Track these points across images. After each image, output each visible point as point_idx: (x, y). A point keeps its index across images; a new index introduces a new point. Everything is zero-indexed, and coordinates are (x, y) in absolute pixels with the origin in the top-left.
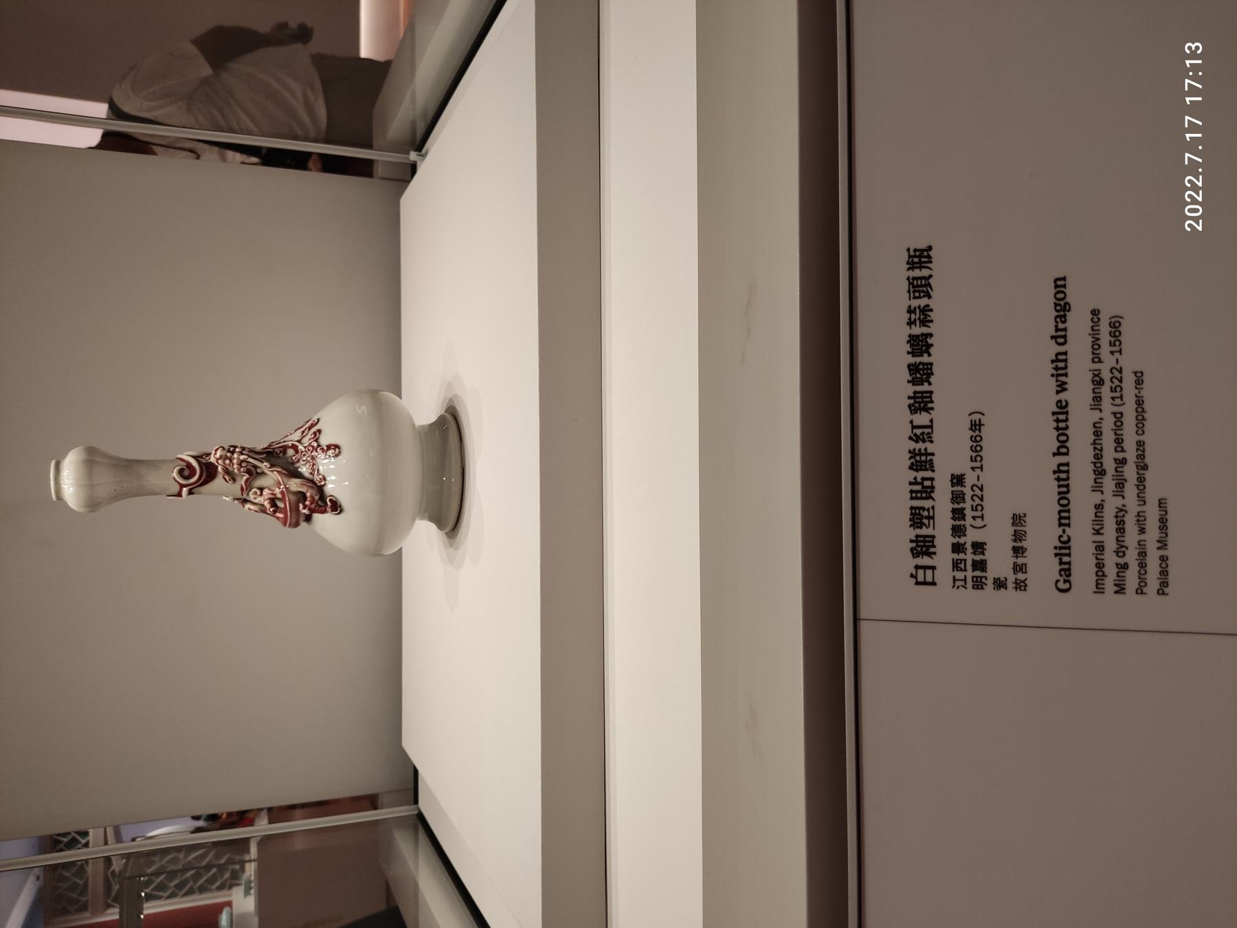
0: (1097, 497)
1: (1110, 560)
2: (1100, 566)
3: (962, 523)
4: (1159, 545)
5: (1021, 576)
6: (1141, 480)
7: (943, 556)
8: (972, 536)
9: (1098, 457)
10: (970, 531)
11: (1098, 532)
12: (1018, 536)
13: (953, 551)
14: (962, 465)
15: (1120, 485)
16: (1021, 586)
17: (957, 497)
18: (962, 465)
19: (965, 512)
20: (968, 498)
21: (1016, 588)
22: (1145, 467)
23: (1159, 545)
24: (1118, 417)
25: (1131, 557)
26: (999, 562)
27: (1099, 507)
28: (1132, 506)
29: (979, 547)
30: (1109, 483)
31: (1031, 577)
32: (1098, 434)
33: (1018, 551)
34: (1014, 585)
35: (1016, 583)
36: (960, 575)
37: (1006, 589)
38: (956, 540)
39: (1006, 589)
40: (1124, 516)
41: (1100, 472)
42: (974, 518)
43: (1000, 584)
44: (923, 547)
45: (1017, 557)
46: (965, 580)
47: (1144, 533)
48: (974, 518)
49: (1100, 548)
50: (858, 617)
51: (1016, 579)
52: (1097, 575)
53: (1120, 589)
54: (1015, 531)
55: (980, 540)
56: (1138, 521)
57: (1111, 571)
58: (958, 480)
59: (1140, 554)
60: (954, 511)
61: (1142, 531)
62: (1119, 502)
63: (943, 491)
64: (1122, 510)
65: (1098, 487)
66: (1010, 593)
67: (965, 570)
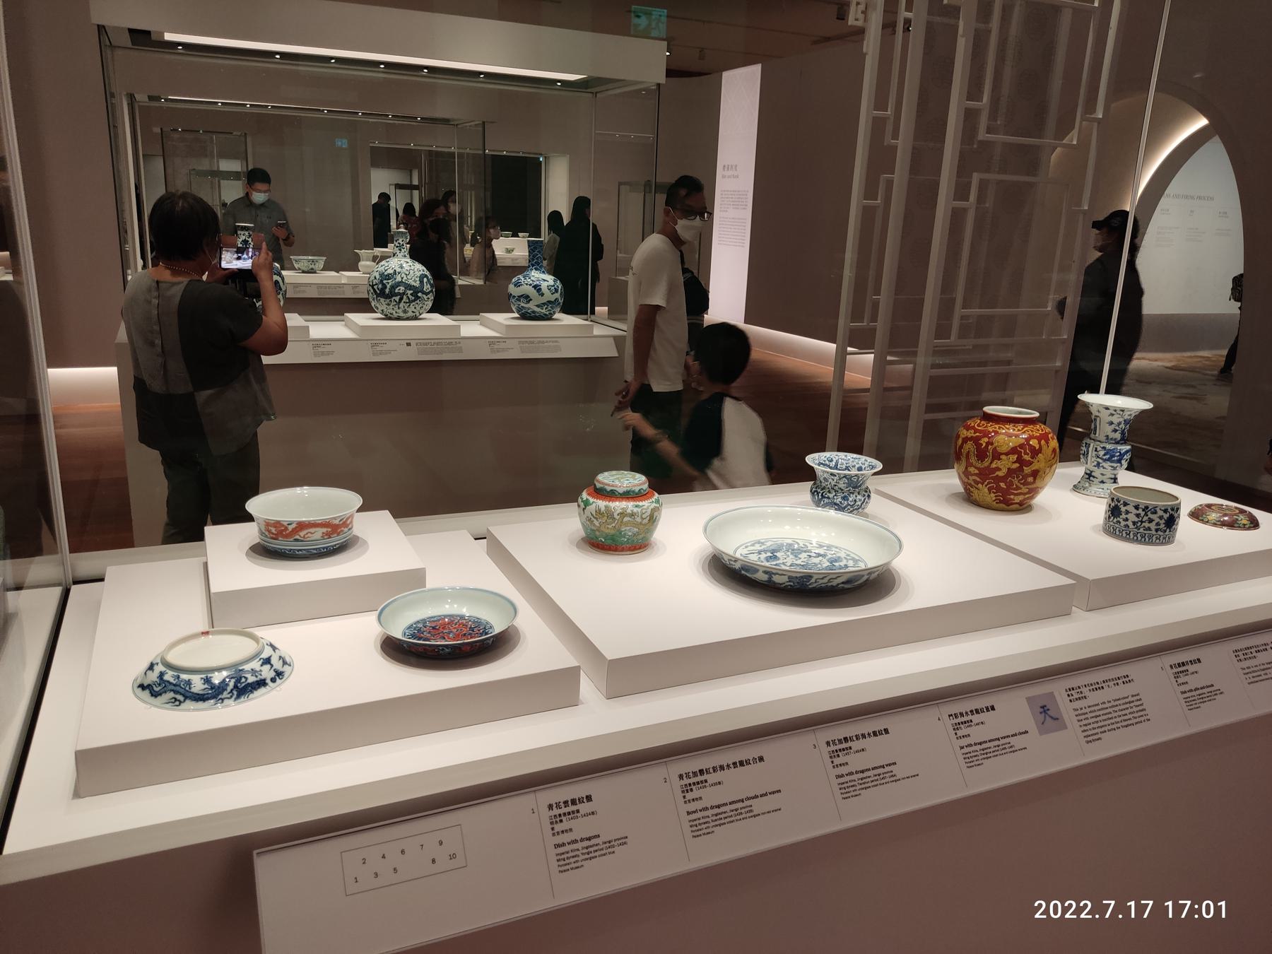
0: (580, 849)
1: (565, 856)
9: (591, 846)
12: (566, 831)
17: (573, 812)
18: (582, 812)
24: (602, 849)
25: (567, 861)
26: (558, 827)
27: (578, 850)
28: (579, 859)
29: (561, 821)
31: (557, 837)
43: (553, 829)
44: (558, 805)
49: (568, 853)
53: (558, 860)
57: (563, 857)
58: (578, 811)
63: (574, 808)
65: (583, 848)
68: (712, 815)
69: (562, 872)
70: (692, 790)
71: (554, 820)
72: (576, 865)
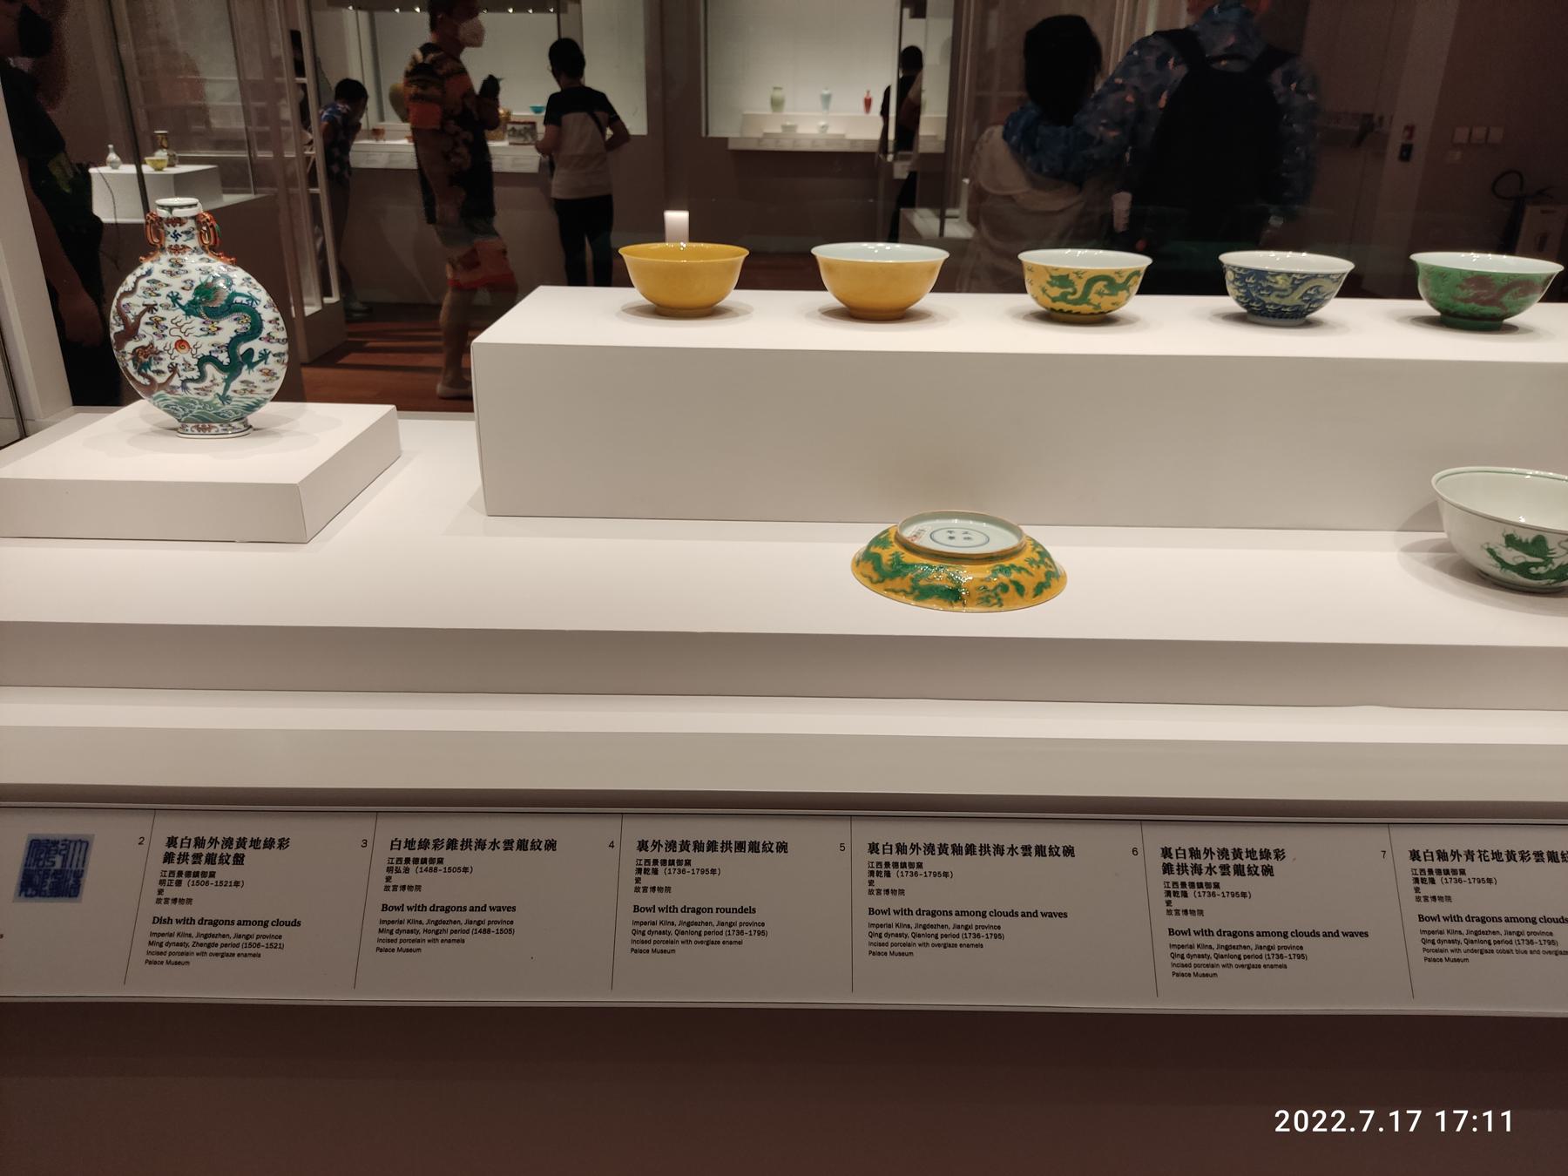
7: (405, 853)
8: (412, 866)
12: (410, 888)
14: (446, 864)
16: (387, 888)
17: (432, 860)
18: (446, 864)
26: (398, 879)
27: (420, 922)
29: (407, 870)
30: (432, 927)
33: (403, 887)
36: (394, 861)
41: (436, 923)
42: (421, 868)
44: (410, 844)
46: (392, 863)
48: (421, 868)
49: (401, 922)
50: (379, 814)
58: (441, 861)
62: (421, 931)
68: (429, 922)
70: (656, 872)
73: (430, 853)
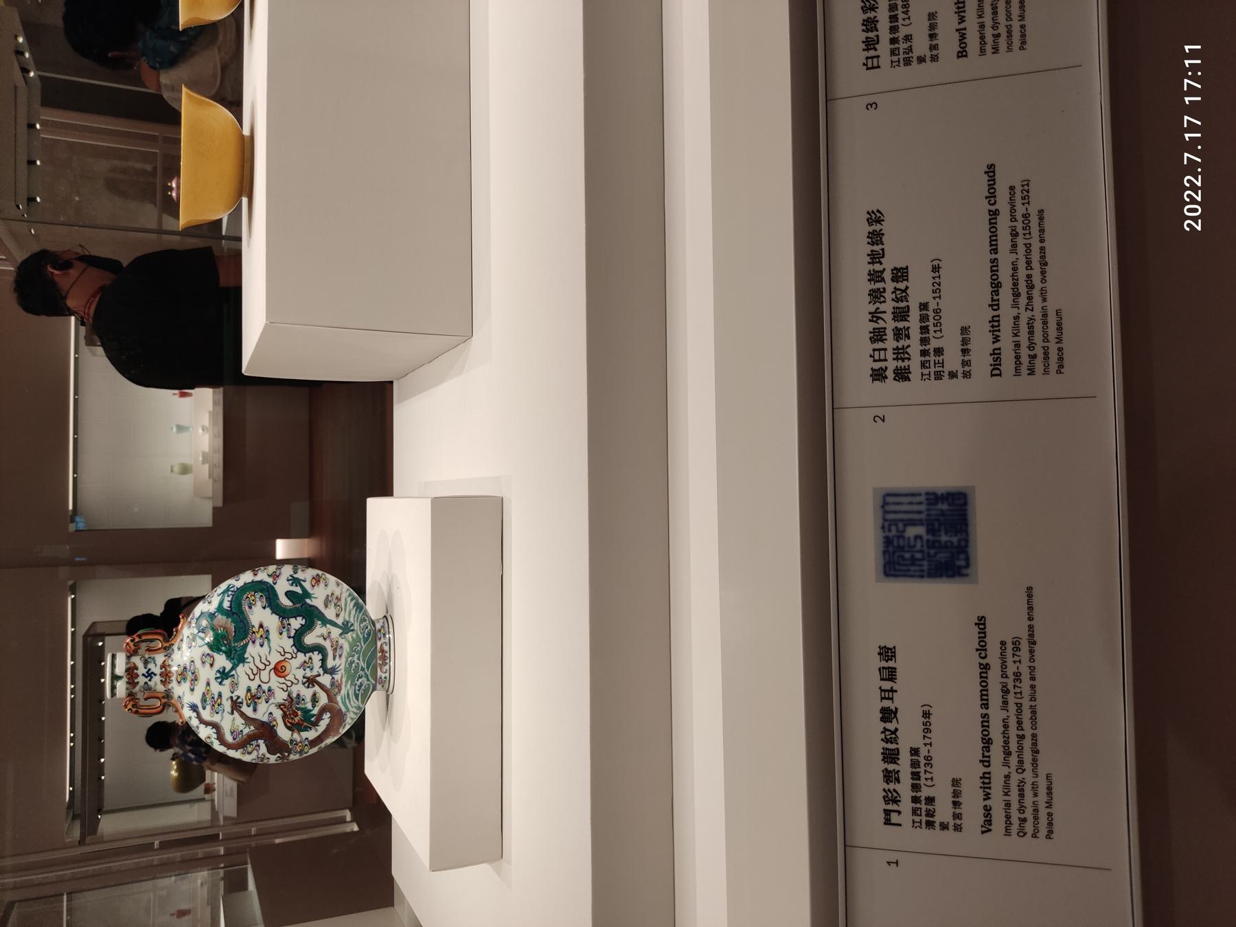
0: (1005, 771)
2: (1008, 817)
3: (918, 782)
4: (1047, 805)
5: (958, 822)
6: (1035, 762)
8: (925, 793)
10: (924, 788)
11: (1006, 794)
12: (956, 794)
13: (912, 802)
15: (1021, 762)
16: (958, 828)
17: (915, 764)
18: (918, 742)
19: (920, 774)
20: (922, 765)
21: (955, 830)
22: (1037, 752)
23: (1047, 805)
25: (1028, 814)
26: (944, 812)
27: (1007, 777)
29: (930, 800)
30: (1014, 760)
31: (965, 822)
32: (1006, 726)
33: (956, 804)
34: (953, 828)
35: (954, 826)
36: (917, 819)
37: (948, 830)
38: (914, 794)
39: (948, 830)
40: (1023, 786)
41: (1008, 753)
42: (926, 779)
43: (944, 827)
44: (891, 798)
45: (955, 808)
46: (921, 822)
47: (1037, 796)
48: (926, 779)
49: (1008, 805)
51: (955, 824)
52: (1006, 823)
54: (954, 790)
55: (931, 795)
56: (1033, 788)
58: (915, 752)
59: (1034, 810)
60: (913, 773)
61: (1036, 795)
62: (1020, 777)
63: (905, 758)
64: (1023, 782)
65: (1006, 764)
66: (951, 832)
67: (921, 815)
69: (1050, 832)
71: (924, 818)
72: (1042, 790)
73: (904, 766)
